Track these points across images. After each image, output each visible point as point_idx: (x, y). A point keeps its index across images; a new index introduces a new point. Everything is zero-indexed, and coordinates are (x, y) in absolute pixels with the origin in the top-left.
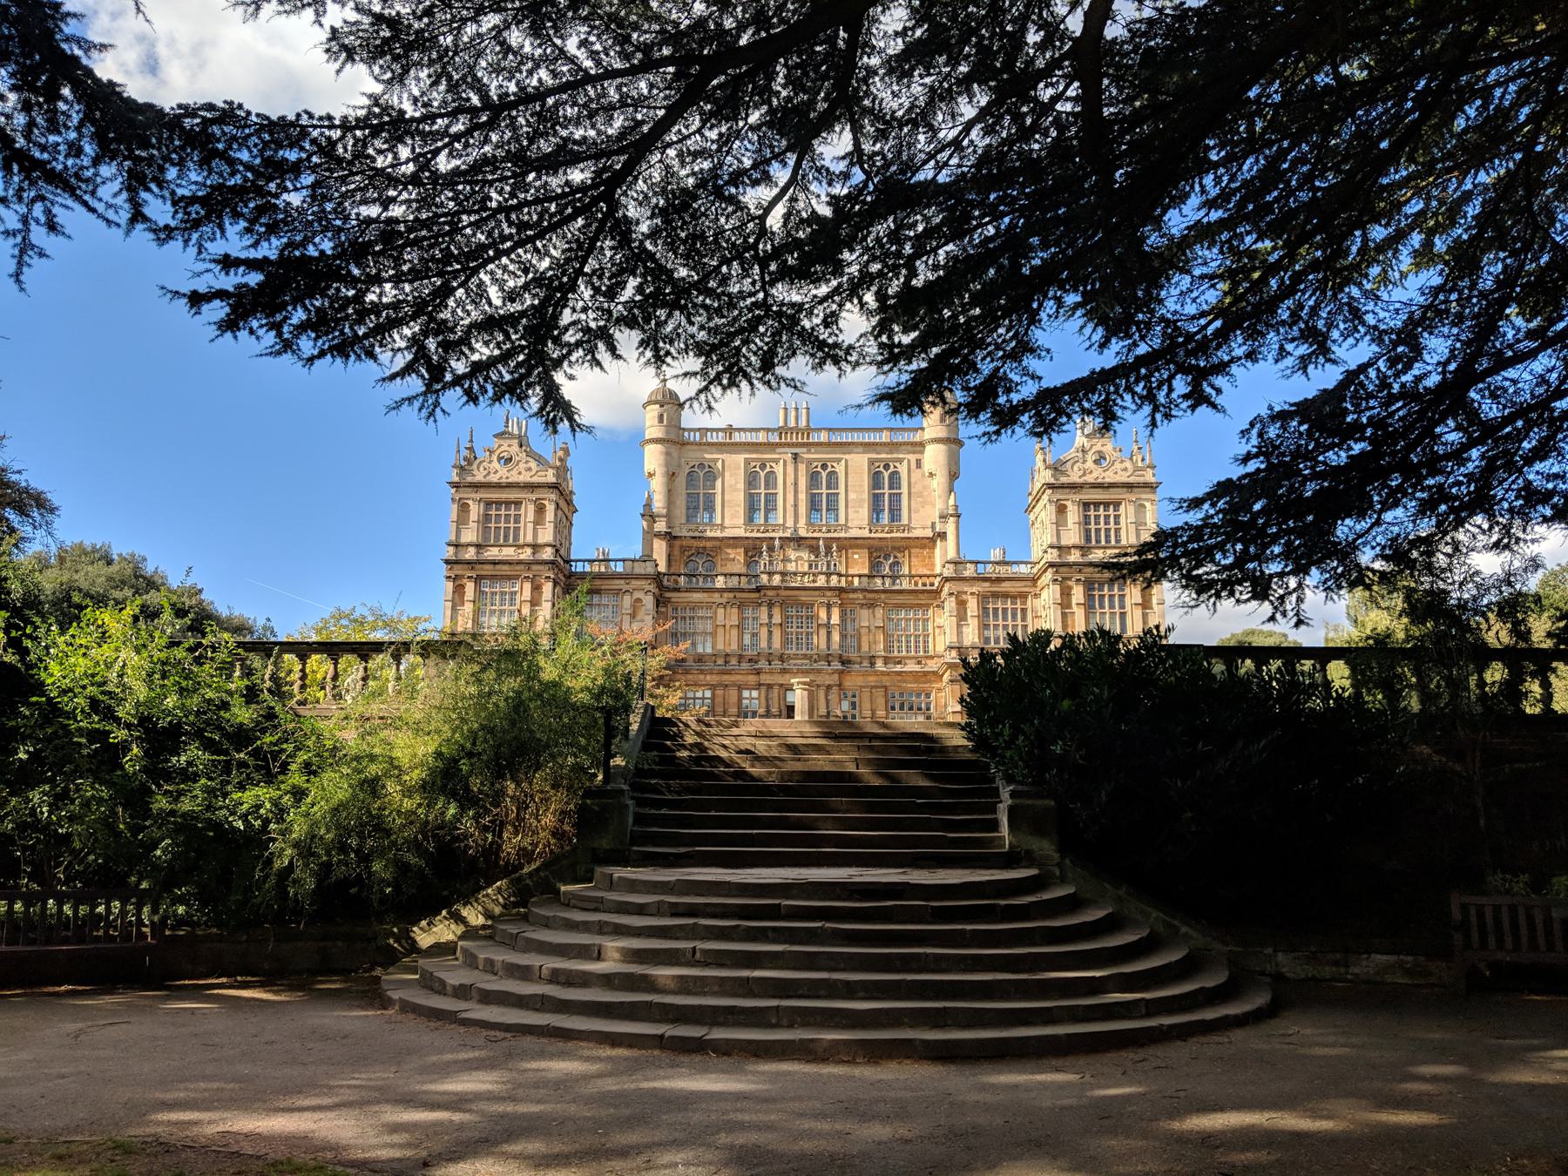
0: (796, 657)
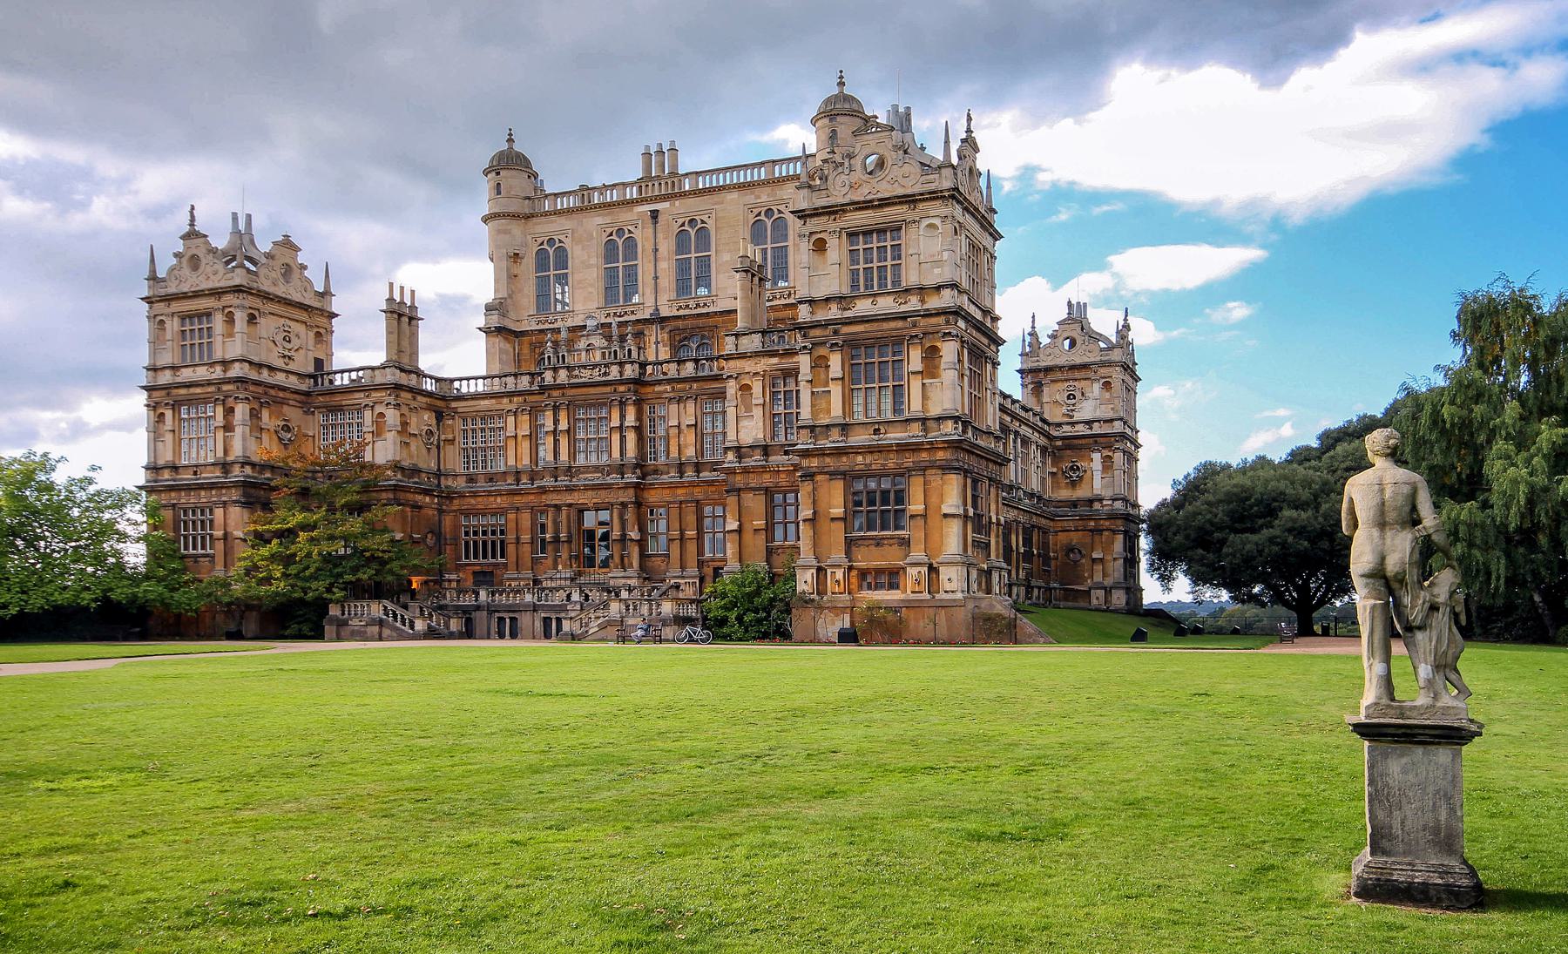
0: (587, 469)
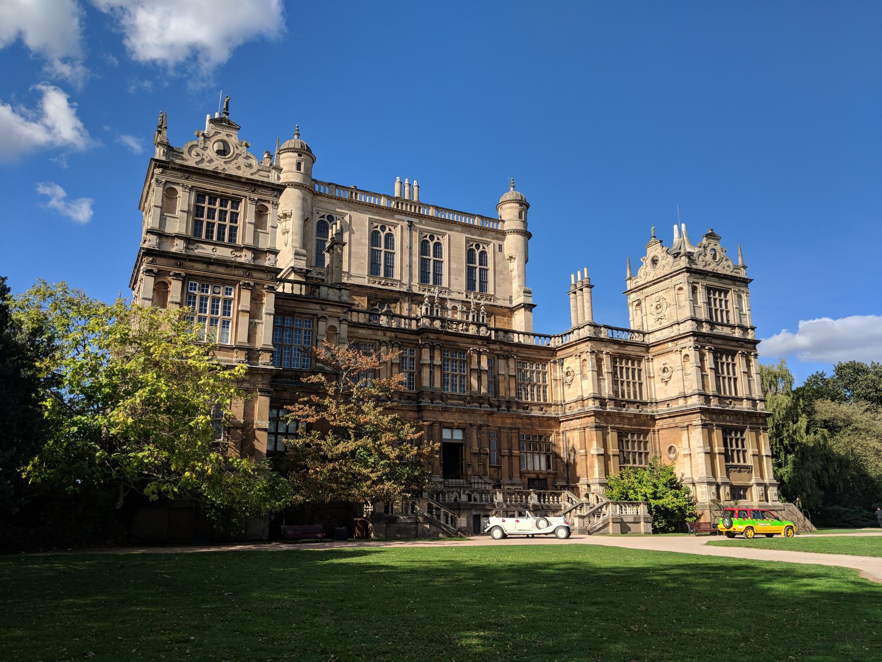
0: (453, 397)
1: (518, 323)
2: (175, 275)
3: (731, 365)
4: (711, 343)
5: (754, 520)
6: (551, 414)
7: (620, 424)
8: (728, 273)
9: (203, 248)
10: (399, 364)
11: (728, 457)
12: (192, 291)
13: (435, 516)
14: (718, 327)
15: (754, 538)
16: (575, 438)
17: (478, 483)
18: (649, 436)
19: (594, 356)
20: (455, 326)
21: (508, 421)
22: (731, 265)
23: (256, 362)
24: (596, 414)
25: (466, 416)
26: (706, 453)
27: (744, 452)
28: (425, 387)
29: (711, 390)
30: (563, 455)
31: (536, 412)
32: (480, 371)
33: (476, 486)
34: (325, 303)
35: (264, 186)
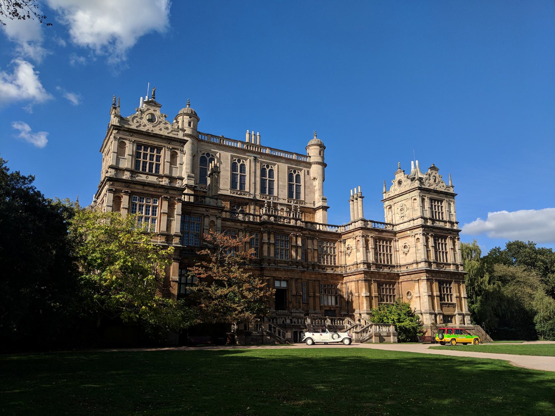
0: (281, 262)
1: (318, 217)
2: (125, 192)
3: (444, 244)
4: (432, 231)
5: (456, 335)
6: (338, 272)
7: (379, 278)
8: (443, 190)
9: (141, 177)
10: (250, 243)
11: (441, 298)
12: (135, 201)
13: (273, 332)
14: (436, 222)
15: (456, 345)
16: (352, 286)
17: (296, 312)
18: (396, 285)
19: (364, 239)
20: (282, 220)
21: (313, 276)
22: (445, 185)
23: (171, 242)
24: (365, 273)
25: (289, 273)
26: (429, 296)
27: (451, 295)
28: (265, 256)
29: (432, 259)
30: (345, 296)
31: (329, 271)
32: (297, 247)
33: (295, 314)
34: (209, 207)
35: (175, 140)
